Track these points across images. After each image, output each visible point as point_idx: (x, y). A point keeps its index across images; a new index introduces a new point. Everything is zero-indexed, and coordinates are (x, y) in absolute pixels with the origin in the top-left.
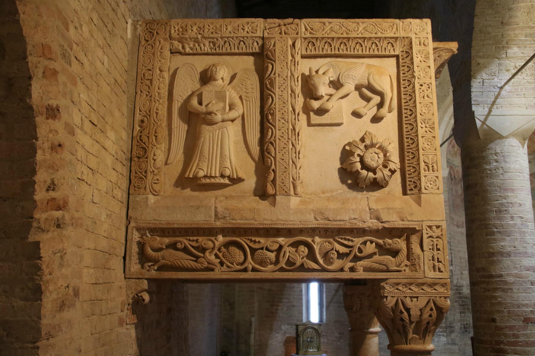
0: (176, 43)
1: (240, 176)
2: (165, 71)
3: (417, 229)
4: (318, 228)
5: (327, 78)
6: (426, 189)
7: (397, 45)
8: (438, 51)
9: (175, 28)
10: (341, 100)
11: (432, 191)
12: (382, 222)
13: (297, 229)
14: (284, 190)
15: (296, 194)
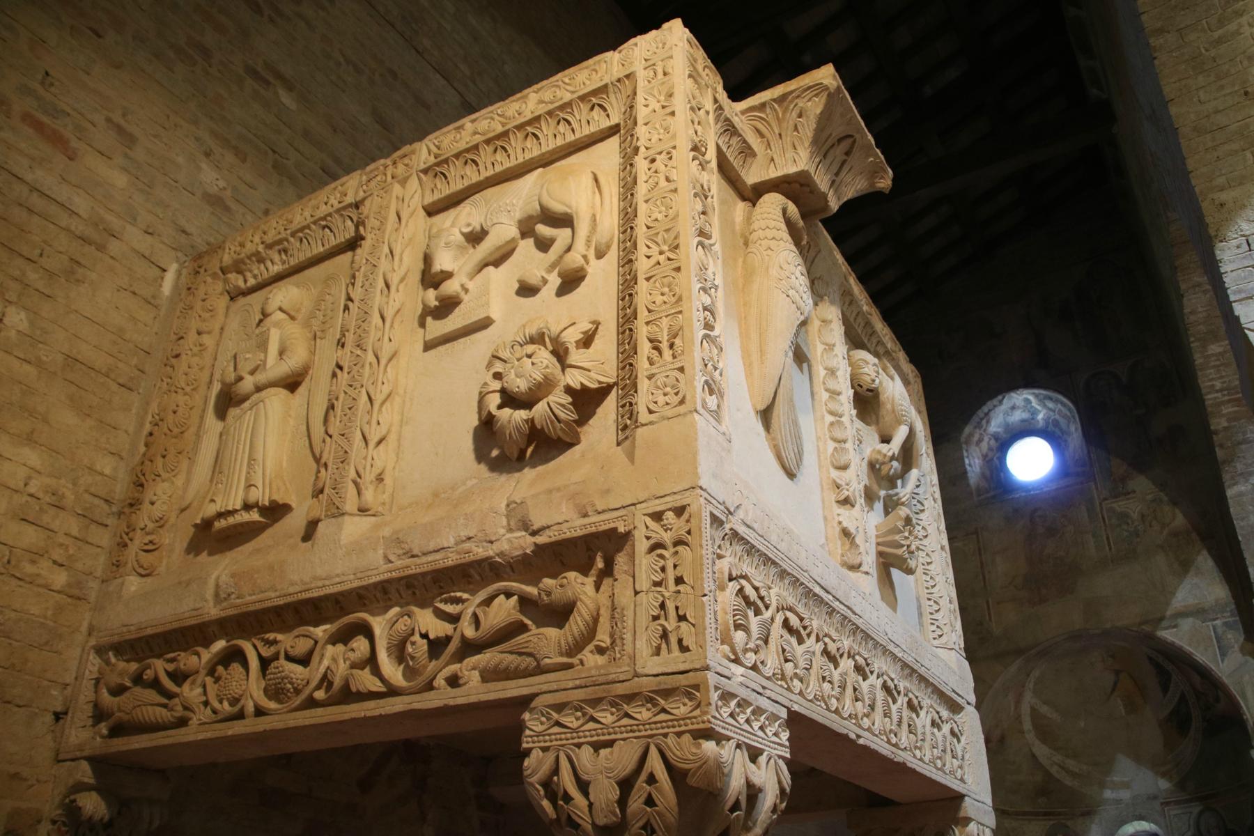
0: (232, 276)
1: (276, 497)
2: (209, 333)
3: (622, 529)
4: (388, 581)
5: (456, 231)
6: (651, 412)
7: (611, 105)
8: (791, 102)
9: (230, 249)
10: (491, 268)
11: (669, 412)
12: (534, 533)
13: (350, 592)
14: (334, 504)
15: (363, 510)
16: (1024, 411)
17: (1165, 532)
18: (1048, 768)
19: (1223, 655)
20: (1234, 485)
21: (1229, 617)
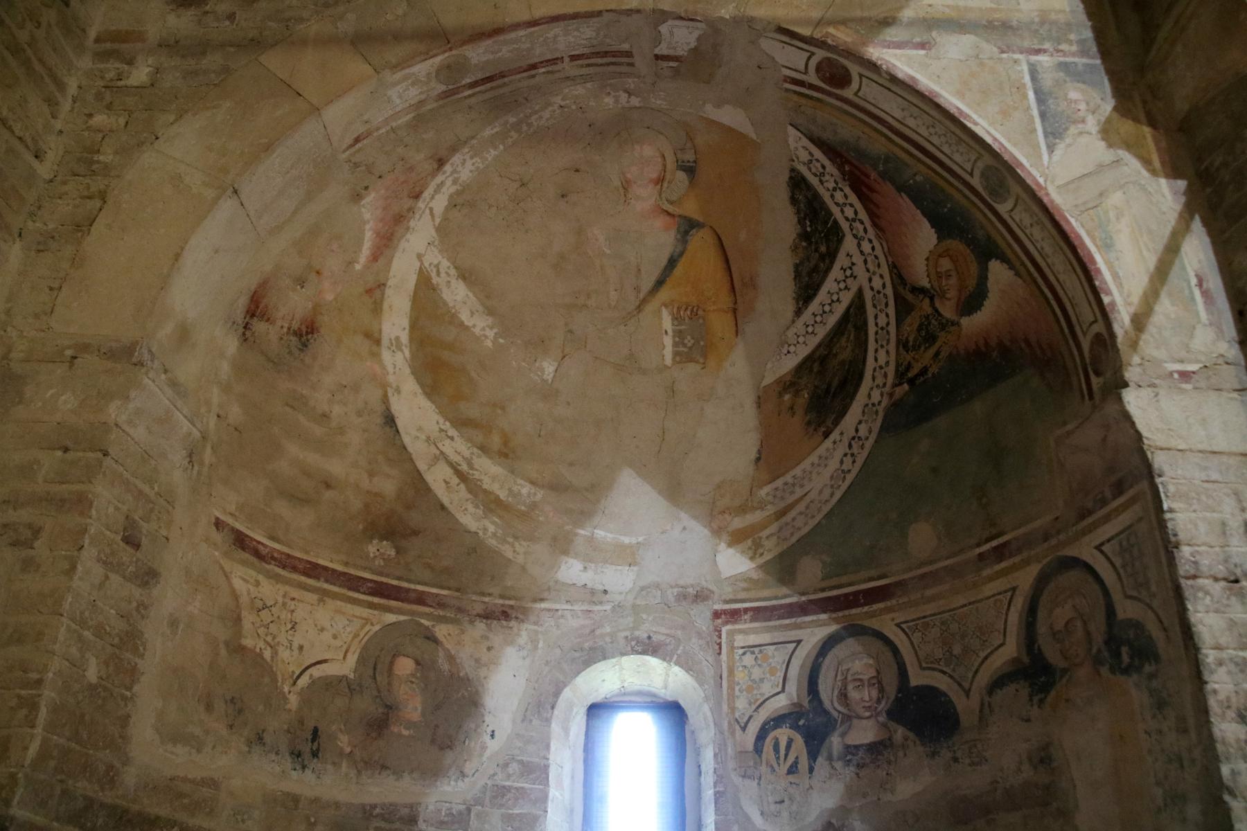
18: (422, 466)
19: (1054, 135)
21: (1073, 55)
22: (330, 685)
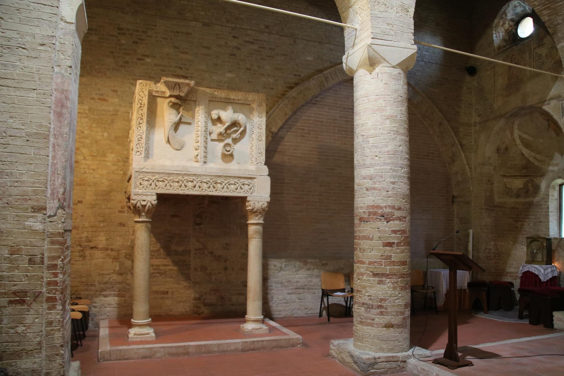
16: (520, 7)
17: (553, 62)
18: (528, 158)
20: (560, 43)
22: (520, 189)
